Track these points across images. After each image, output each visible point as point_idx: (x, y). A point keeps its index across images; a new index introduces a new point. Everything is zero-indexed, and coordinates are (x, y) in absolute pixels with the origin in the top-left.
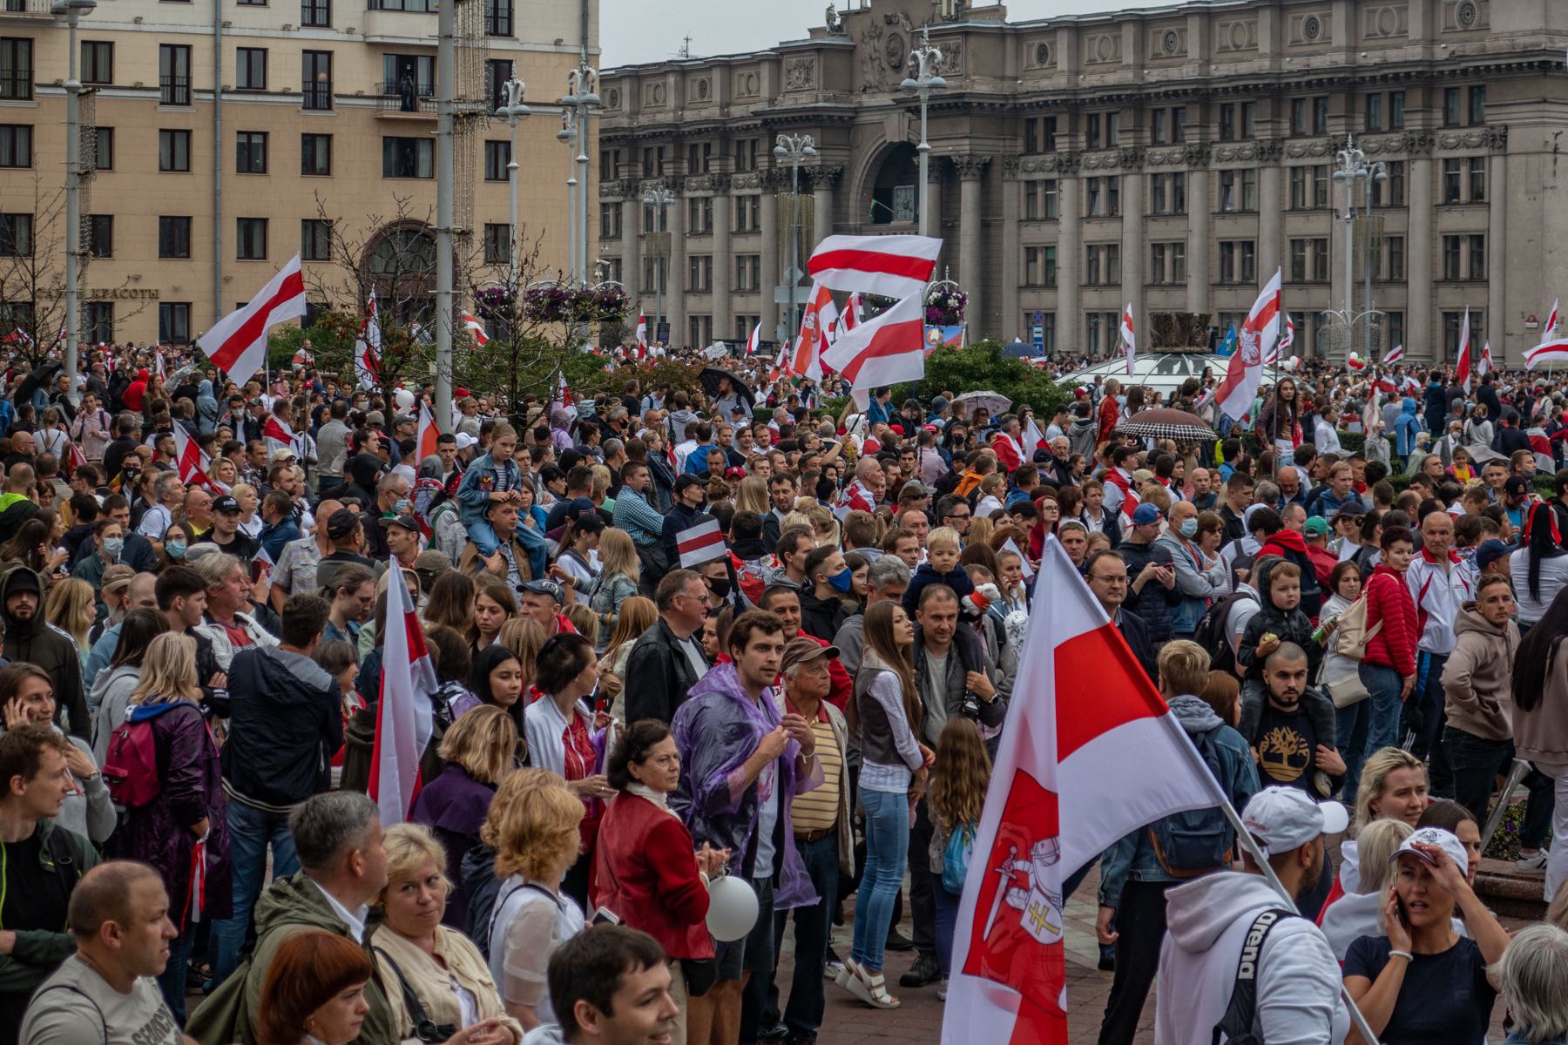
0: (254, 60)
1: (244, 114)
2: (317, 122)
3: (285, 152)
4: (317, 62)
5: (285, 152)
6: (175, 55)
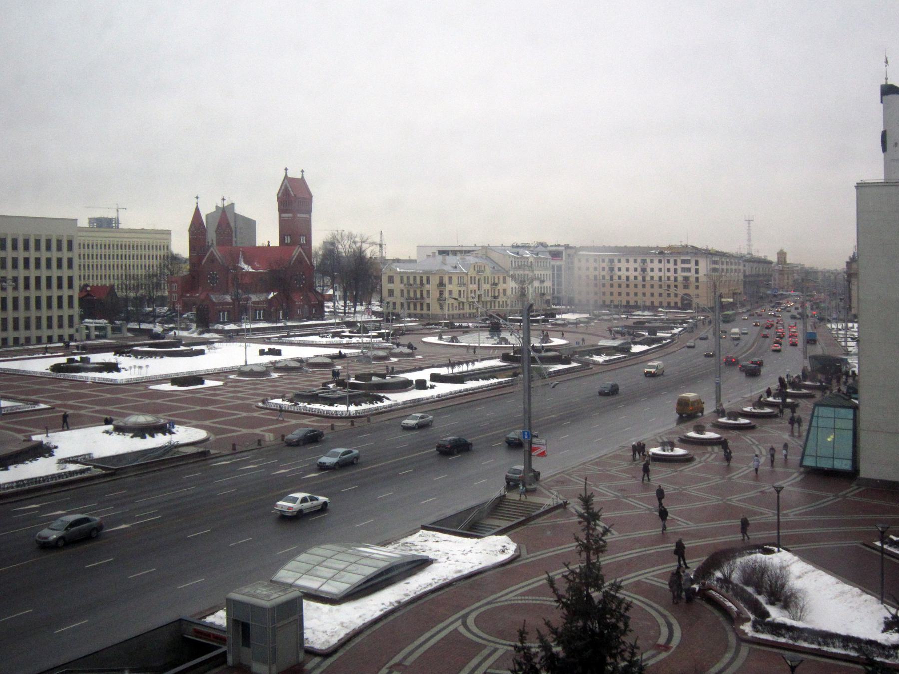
4: (676, 278)
6: (660, 278)
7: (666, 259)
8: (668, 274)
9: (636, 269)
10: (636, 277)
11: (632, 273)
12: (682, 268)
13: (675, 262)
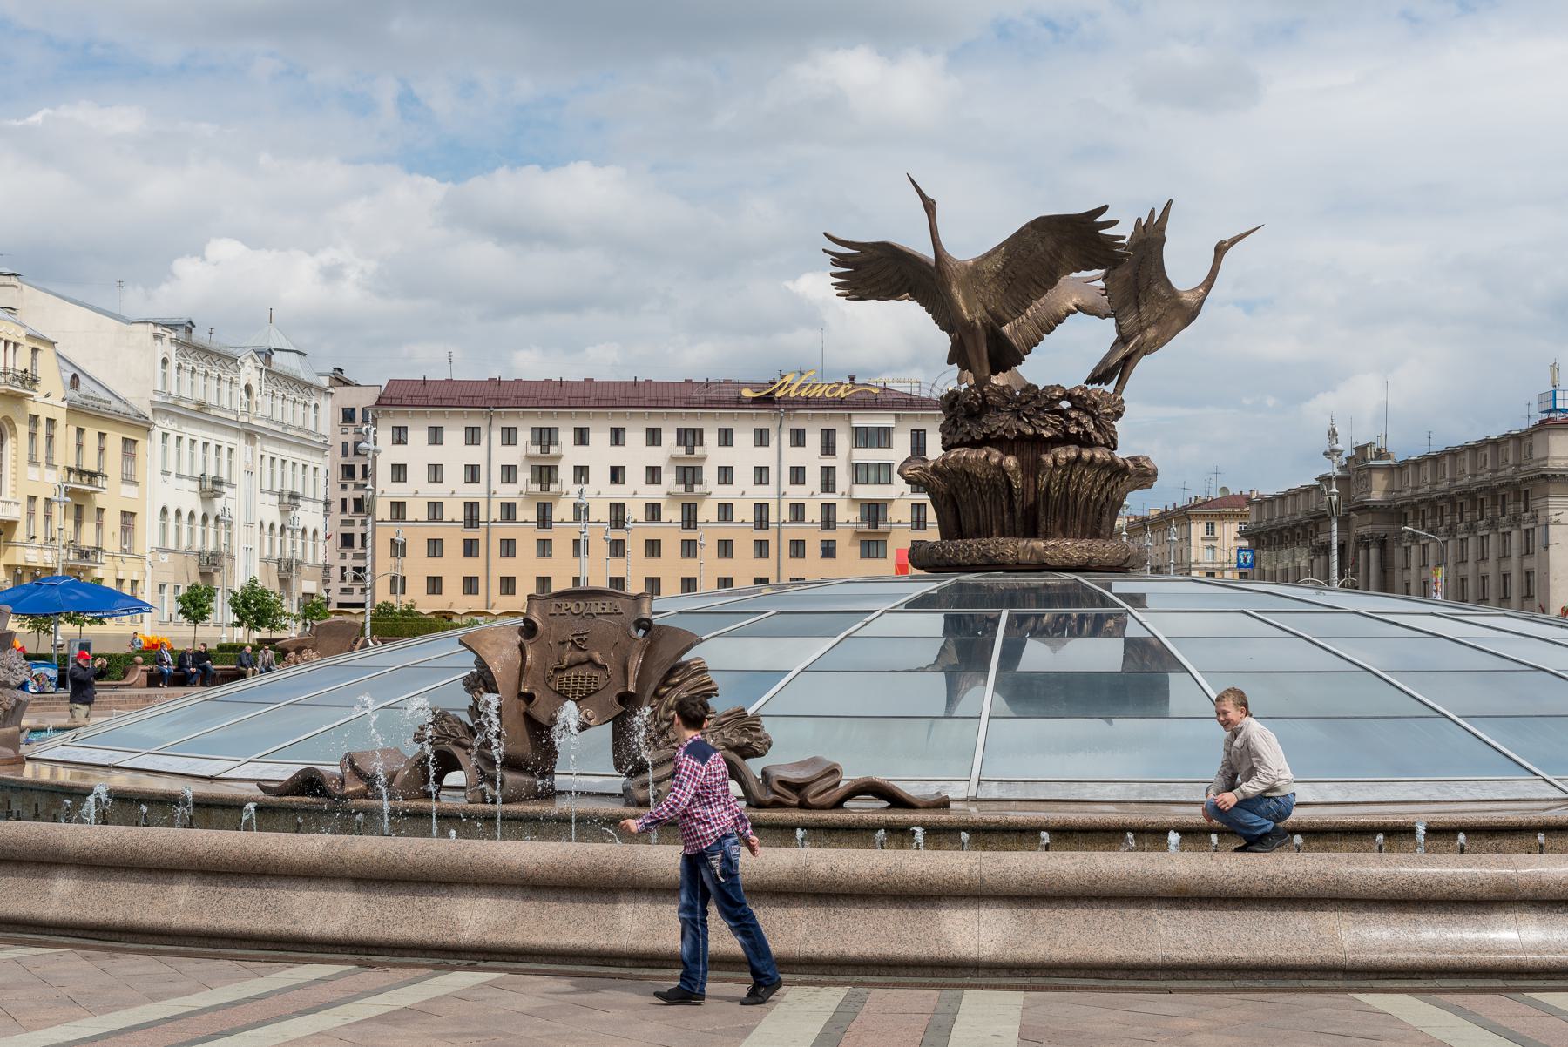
0: (798, 510)
1: (794, 532)
2: (828, 535)
3: (813, 549)
4: (828, 509)
5: (813, 549)
6: (761, 509)
7: (789, 425)
8: (795, 493)
9: (654, 474)
10: (654, 511)
11: (636, 496)
12: (856, 467)
13: (828, 447)
